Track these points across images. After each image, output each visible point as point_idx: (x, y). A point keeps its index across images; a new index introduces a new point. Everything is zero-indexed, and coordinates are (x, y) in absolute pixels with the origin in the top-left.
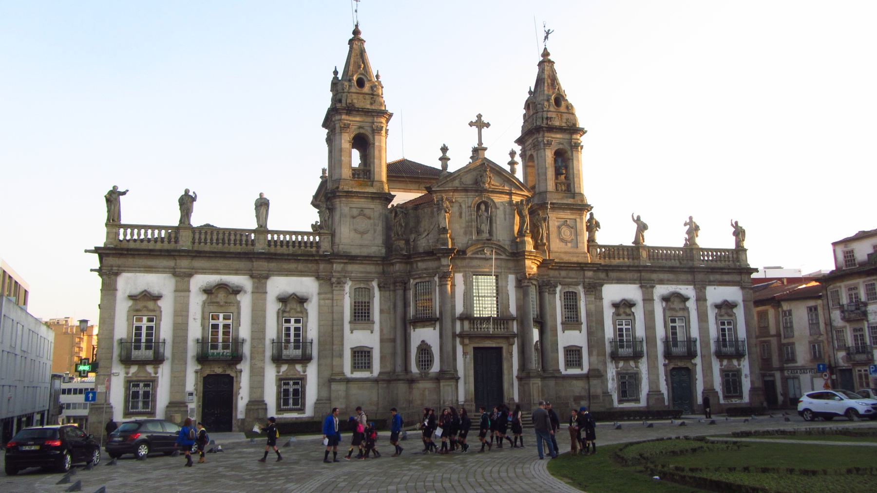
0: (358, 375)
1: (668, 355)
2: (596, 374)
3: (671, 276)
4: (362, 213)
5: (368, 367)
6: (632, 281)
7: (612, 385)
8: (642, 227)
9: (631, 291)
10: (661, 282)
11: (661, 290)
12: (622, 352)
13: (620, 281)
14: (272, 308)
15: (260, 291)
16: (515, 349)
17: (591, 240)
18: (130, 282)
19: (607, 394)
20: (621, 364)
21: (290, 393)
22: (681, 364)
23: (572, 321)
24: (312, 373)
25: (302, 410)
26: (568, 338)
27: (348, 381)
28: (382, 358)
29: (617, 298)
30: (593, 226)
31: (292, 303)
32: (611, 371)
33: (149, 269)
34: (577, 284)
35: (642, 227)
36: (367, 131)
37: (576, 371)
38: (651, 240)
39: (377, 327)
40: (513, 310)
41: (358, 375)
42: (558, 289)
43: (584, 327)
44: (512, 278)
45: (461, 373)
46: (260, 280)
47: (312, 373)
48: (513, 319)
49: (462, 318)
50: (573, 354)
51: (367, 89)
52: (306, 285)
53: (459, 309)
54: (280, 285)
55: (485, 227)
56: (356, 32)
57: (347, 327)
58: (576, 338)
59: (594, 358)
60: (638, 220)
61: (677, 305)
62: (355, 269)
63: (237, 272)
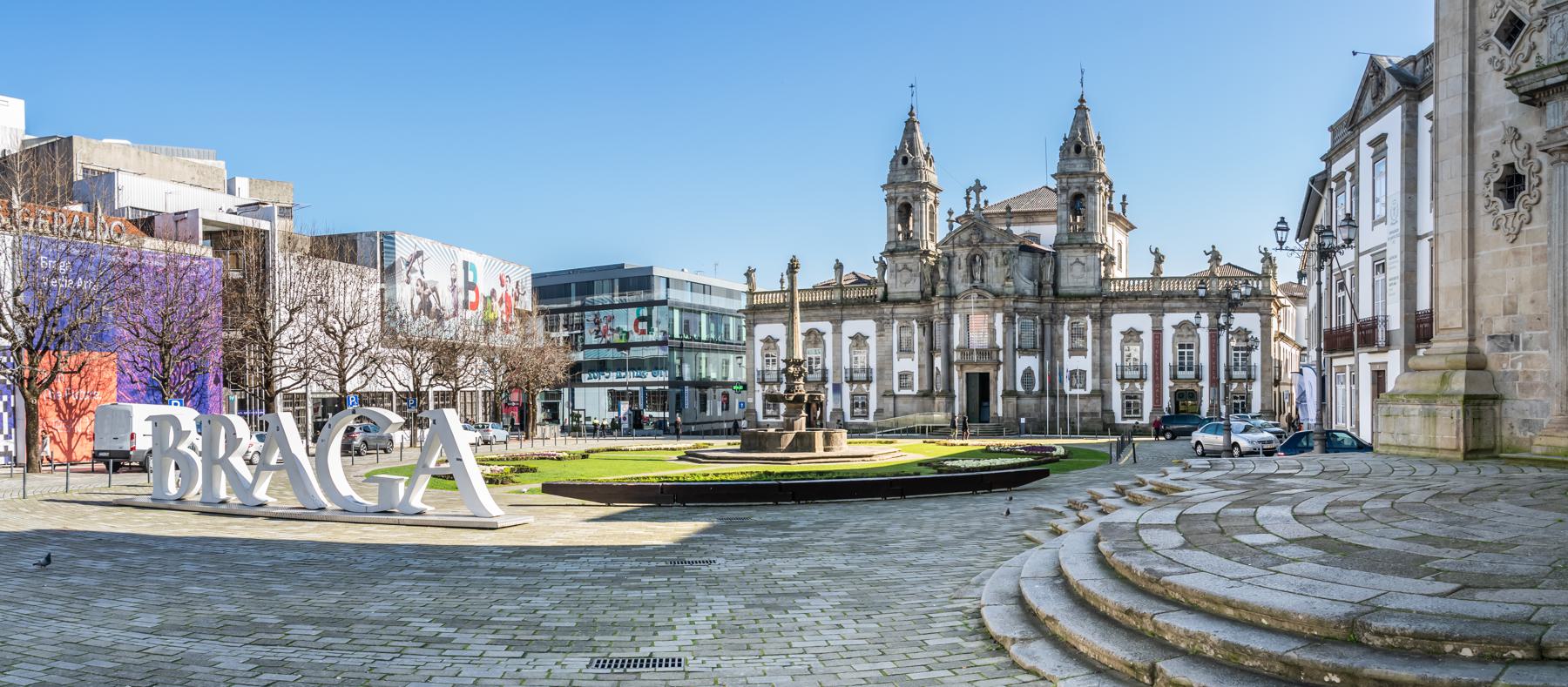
0: (903, 392)
1: (1174, 378)
2: (1102, 394)
3: (1182, 304)
4: (905, 267)
5: (911, 387)
6: (1144, 310)
7: (1117, 405)
8: (1159, 260)
9: (1142, 322)
10: (1172, 310)
11: (1170, 320)
12: (1128, 374)
13: (1130, 310)
14: (847, 343)
15: (837, 331)
16: (1001, 373)
17: (1107, 274)
18: (762, 330)
19: (1111, 413)
20: (1127, 385)
21: (860, 403)
22: (1186, 387)
23: (1077, 351)
24: (873, 390)
25: (866, 417)
26: (1071, 363)
27: (895, 397)
28: (920, 380)
29: (1125, 329)
30: (1109, 260)
31: (859, 340)
32: (1117, 391)
33: (770, 321)
34: (1085, 314)
35: (1159, 260)
36: (910, 200)
37: (1082, 392)
38: (1167, 271)
39: (916, 355)
40: (999, 342)
41: (903, 392)
42: (1067, 318)
43: (1089, 353)
44: (999, 316)
45: (957, 393)
46: (837, 323)
47: (873, 390)
48: (998, 350)
49: (959, 349)
50: (1077, 376)
51: (910, 164)
52: (867, 327)
53: (956, 343)
54: (851, 327)
55: (978, 276)
56: (911, 114)
57: (895, 356)
58: (1084, 363)
59: (1097, 381)
60: (1156, 252)
61: (1184, 332)
62: (900, 310)
63: (822, 319)
